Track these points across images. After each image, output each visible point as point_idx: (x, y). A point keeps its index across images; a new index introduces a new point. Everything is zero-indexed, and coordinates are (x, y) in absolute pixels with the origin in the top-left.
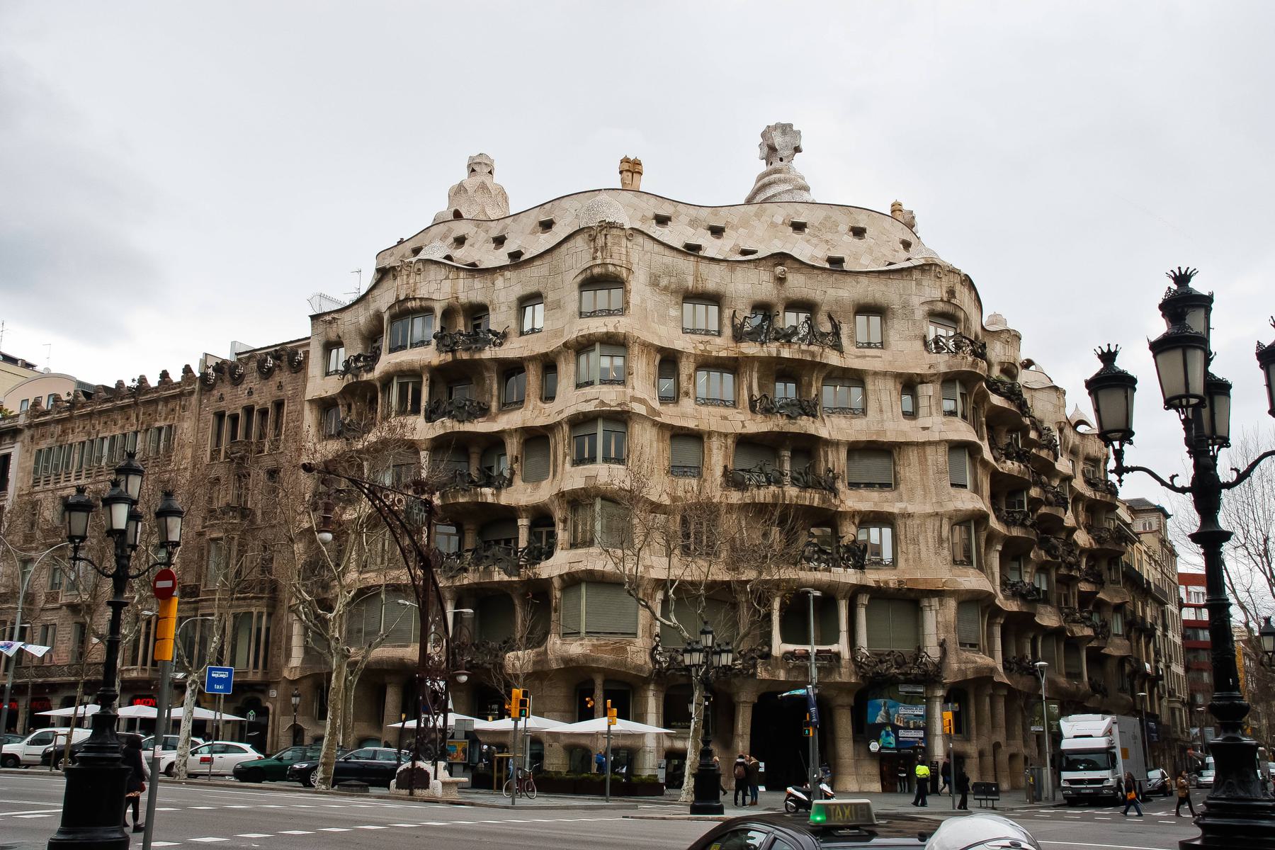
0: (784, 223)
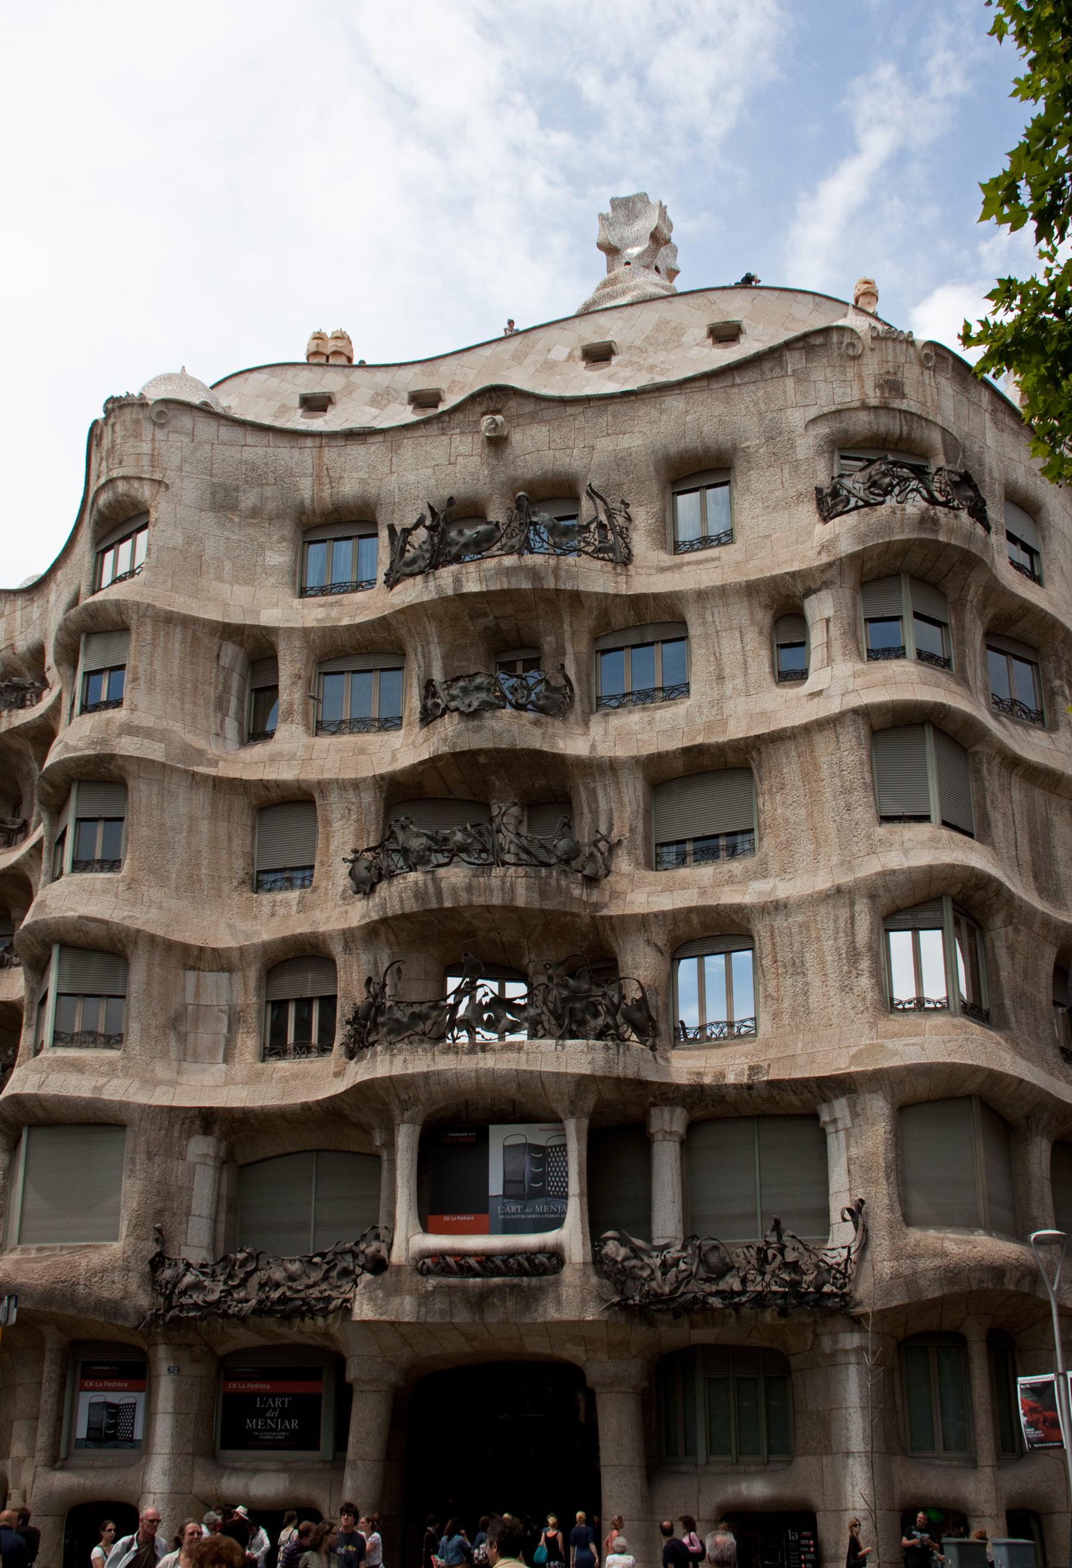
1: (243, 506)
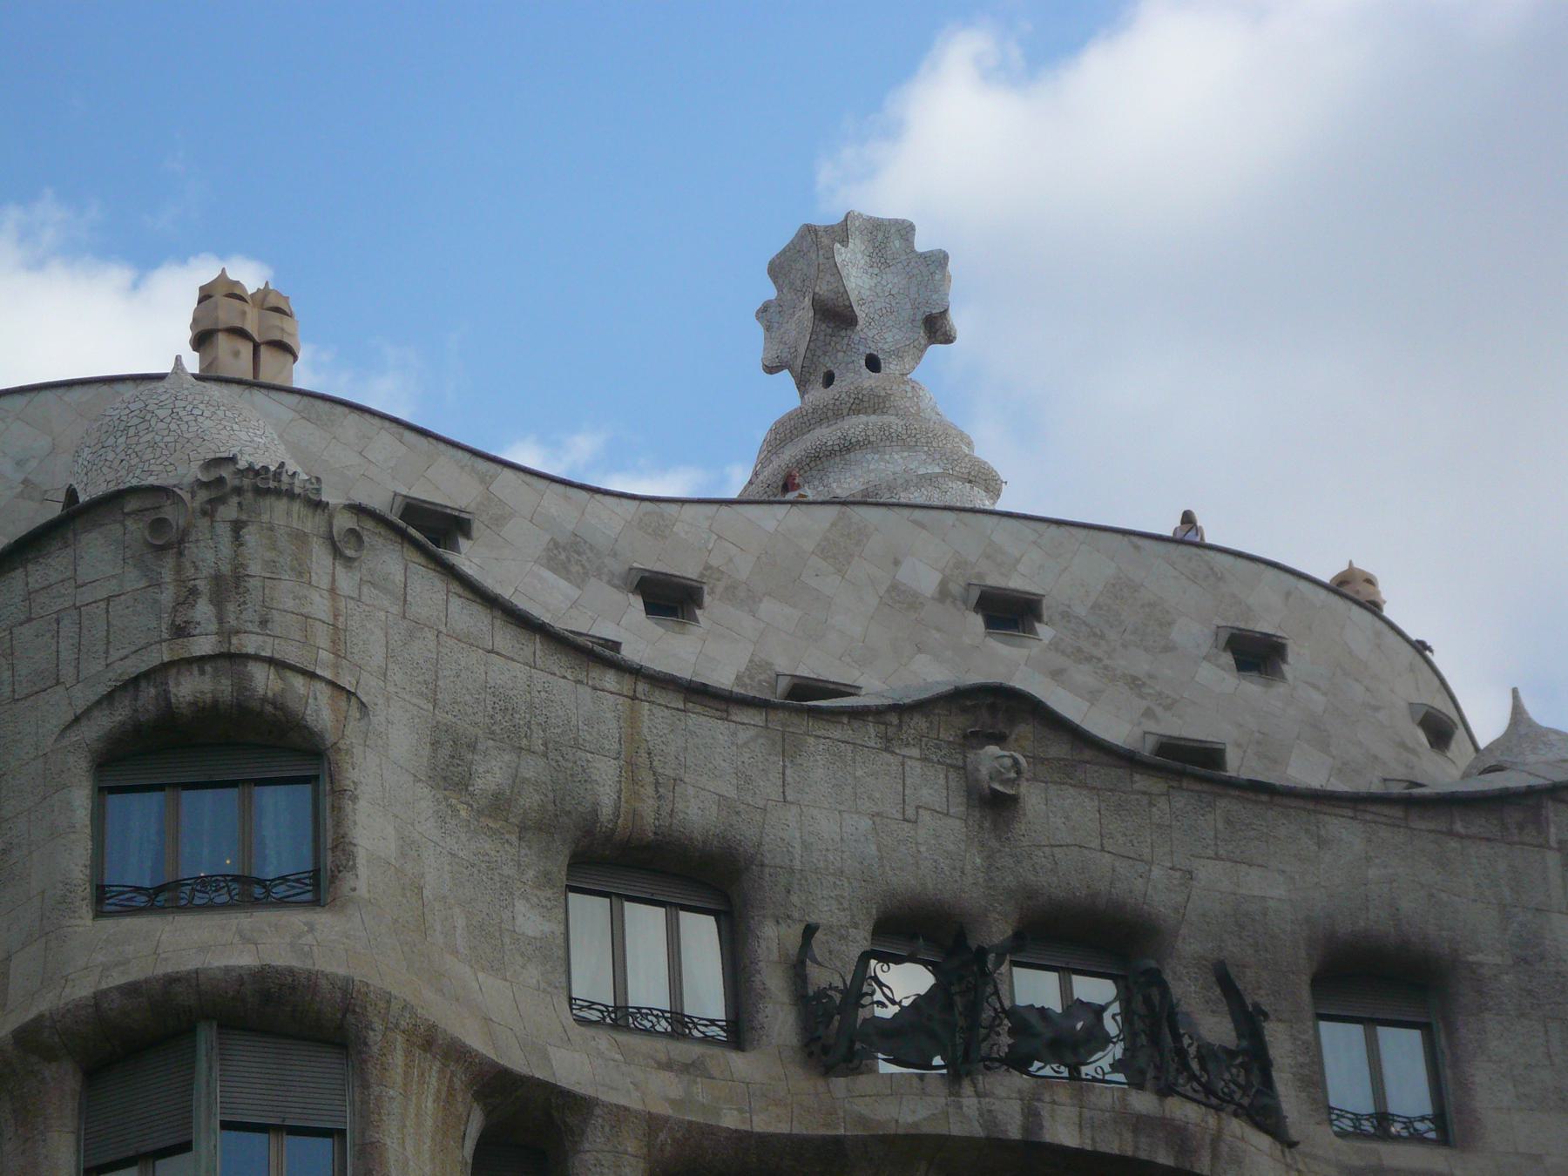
0: (943, 594)
1: (479, 784)
